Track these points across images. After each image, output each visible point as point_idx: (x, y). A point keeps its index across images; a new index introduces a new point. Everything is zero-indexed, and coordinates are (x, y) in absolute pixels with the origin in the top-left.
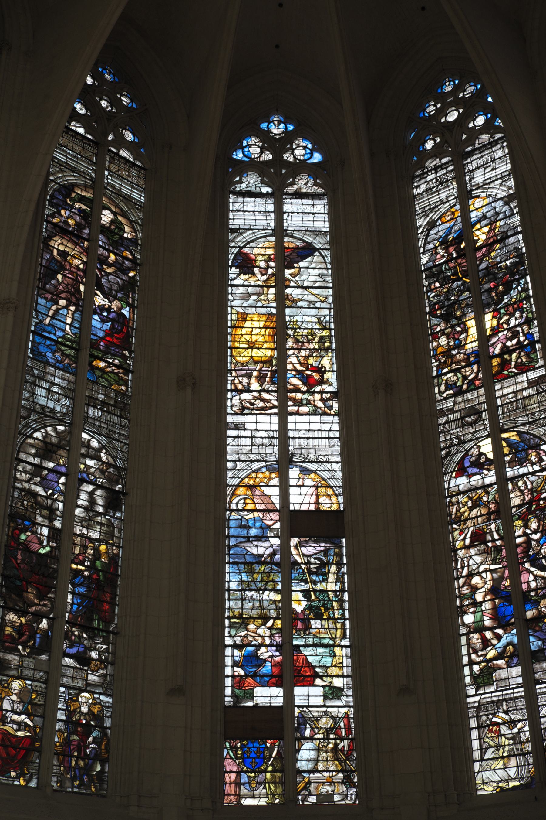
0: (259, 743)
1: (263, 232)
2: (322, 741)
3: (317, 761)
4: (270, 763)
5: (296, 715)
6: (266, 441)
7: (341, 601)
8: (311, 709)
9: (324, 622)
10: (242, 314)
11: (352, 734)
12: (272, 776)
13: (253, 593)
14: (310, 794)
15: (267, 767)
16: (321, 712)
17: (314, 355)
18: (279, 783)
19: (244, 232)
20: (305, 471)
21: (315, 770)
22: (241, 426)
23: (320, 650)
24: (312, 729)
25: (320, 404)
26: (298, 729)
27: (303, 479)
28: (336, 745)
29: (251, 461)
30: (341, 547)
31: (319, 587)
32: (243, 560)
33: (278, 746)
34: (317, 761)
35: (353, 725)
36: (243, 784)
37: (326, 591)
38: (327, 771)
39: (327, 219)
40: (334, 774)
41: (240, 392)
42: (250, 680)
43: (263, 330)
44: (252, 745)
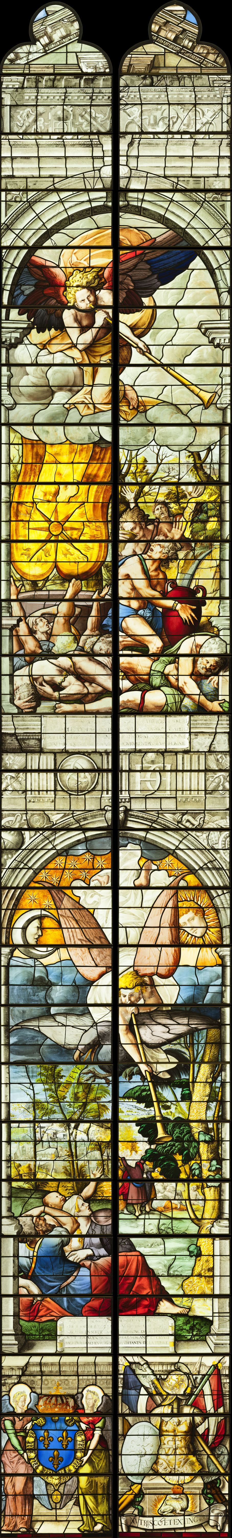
0: (65, 1422)
1: (84, 197)
6: (85, 779)
7: (215, 1142)
9: (181, 1187)
10: (33, 443)
11: (223, 1405)
13: (56, 1126)
16: (167, 1364)
17: (181, 554)
19: (39, 200)
20: (155, 853)
22: (32, 742)
23: (172, 1244)
25: (191, 687)
27: (148, 870)
28: (193, 1427)
29: (54, 830)
30: (221, 1026)
31: (173, 1113)
32: (37, 1058)
37: (187, 1122)
39: (226, 152)
40: (188, 1479)
41: (32, 658)
42: (49, 1303)
43: (84, 488)
44: (53, 1426)
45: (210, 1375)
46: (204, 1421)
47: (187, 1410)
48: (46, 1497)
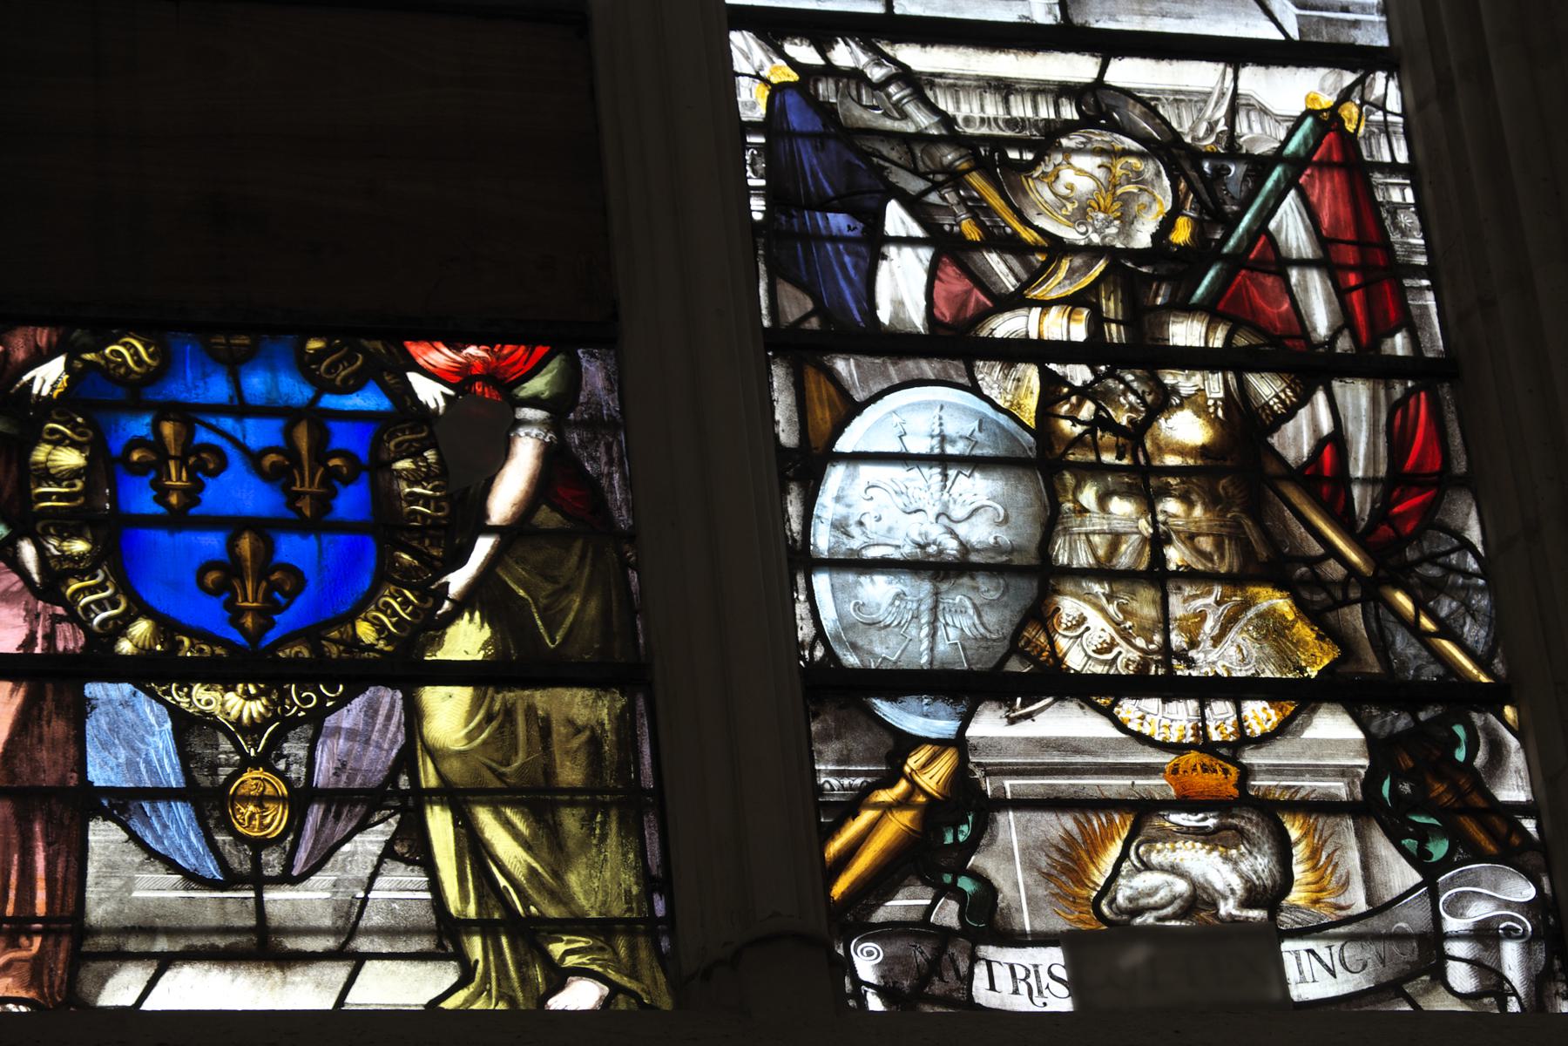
2: (1079, 374)
3: (1034, 577)
4: (457, 581)
5: (752, 101)
8: (915, 57)
11: (1411, 324)
12: (497, 726)
14: (988, 923)
15: (436, 627)
18: (591, 798)
21: (1022, 672)
24: (948, 250)
26: (786, 246)
33: (558, 407)
34: (1034, 577)
35: (1411, 239)
36: (122, 804)
38: (1170, 689)
45: (1297, 164)
46: (1305, 399)
47: (1186, 333)
48: (182, 811)
